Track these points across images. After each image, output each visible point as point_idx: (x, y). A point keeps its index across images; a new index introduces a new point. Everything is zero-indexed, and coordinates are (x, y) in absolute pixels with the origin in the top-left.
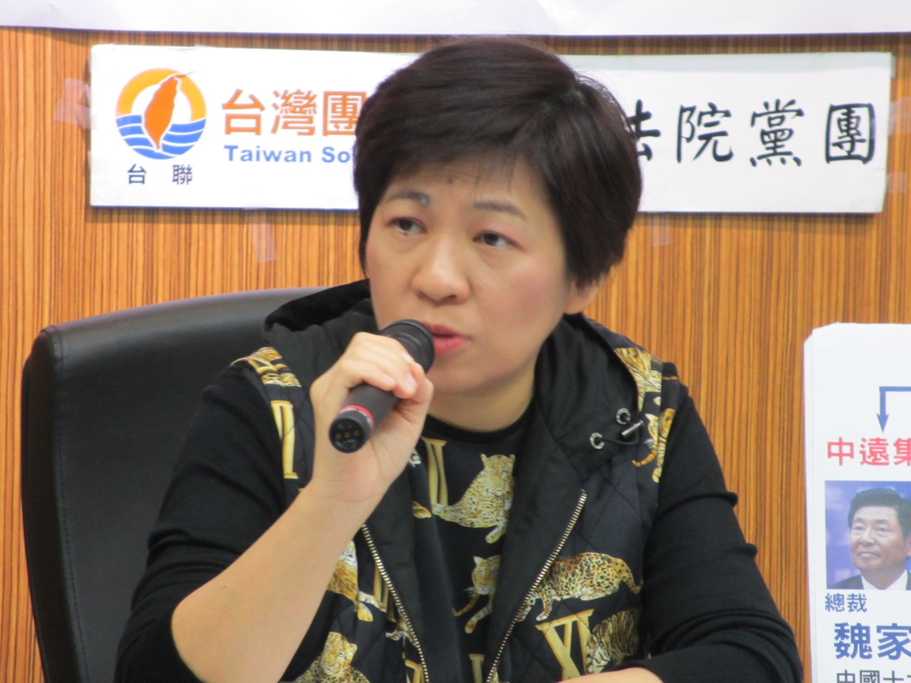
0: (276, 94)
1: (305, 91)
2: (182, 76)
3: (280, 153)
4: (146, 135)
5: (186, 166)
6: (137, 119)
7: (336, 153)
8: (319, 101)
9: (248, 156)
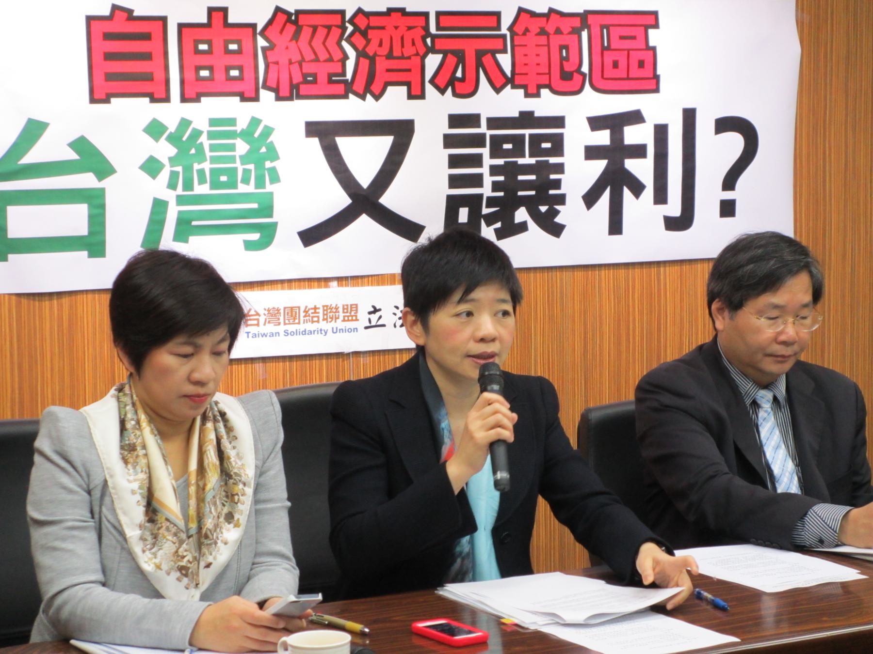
8: (282, 311)
9: (255, 336)
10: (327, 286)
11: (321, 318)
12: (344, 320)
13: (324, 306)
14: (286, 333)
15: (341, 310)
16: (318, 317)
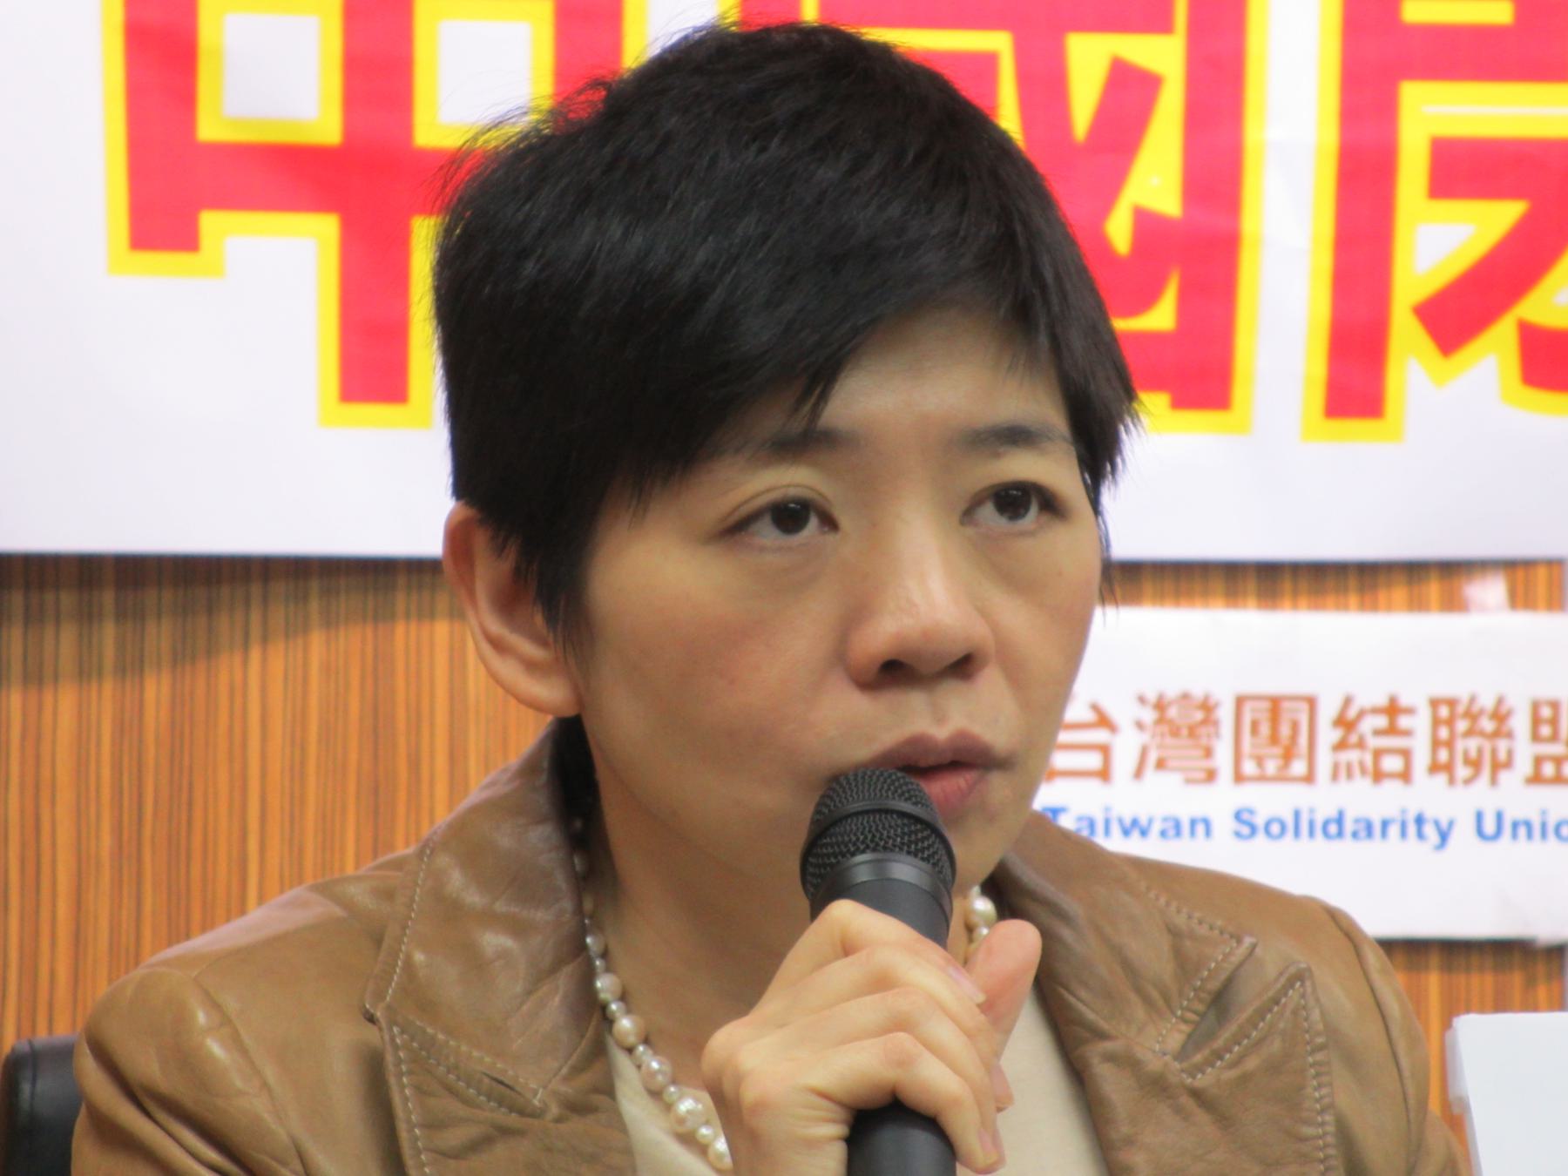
0: (1142, 700)
1: (1198, 692)
3: (1150, 821)
7: (1260, 821)
8: (1225, 715)
10: (1454, 603)
11: (1421, 759)
12: (1536, 779)
13: (1435, 703)
14: (1246, 825)
15: (1520, 723)
16: (1406, 754)
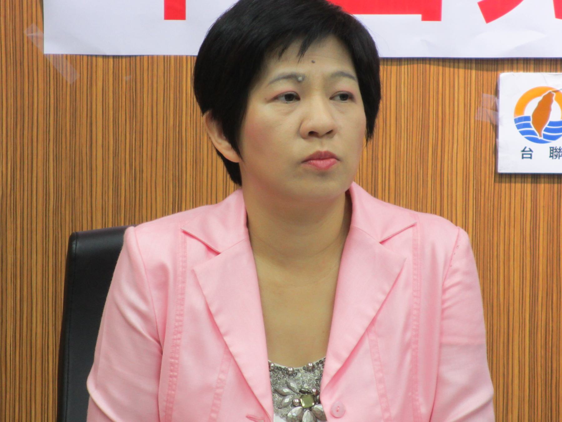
2: (556, 91)
4: (533, 129)
5: (558, 147)
6: (527, 118)
